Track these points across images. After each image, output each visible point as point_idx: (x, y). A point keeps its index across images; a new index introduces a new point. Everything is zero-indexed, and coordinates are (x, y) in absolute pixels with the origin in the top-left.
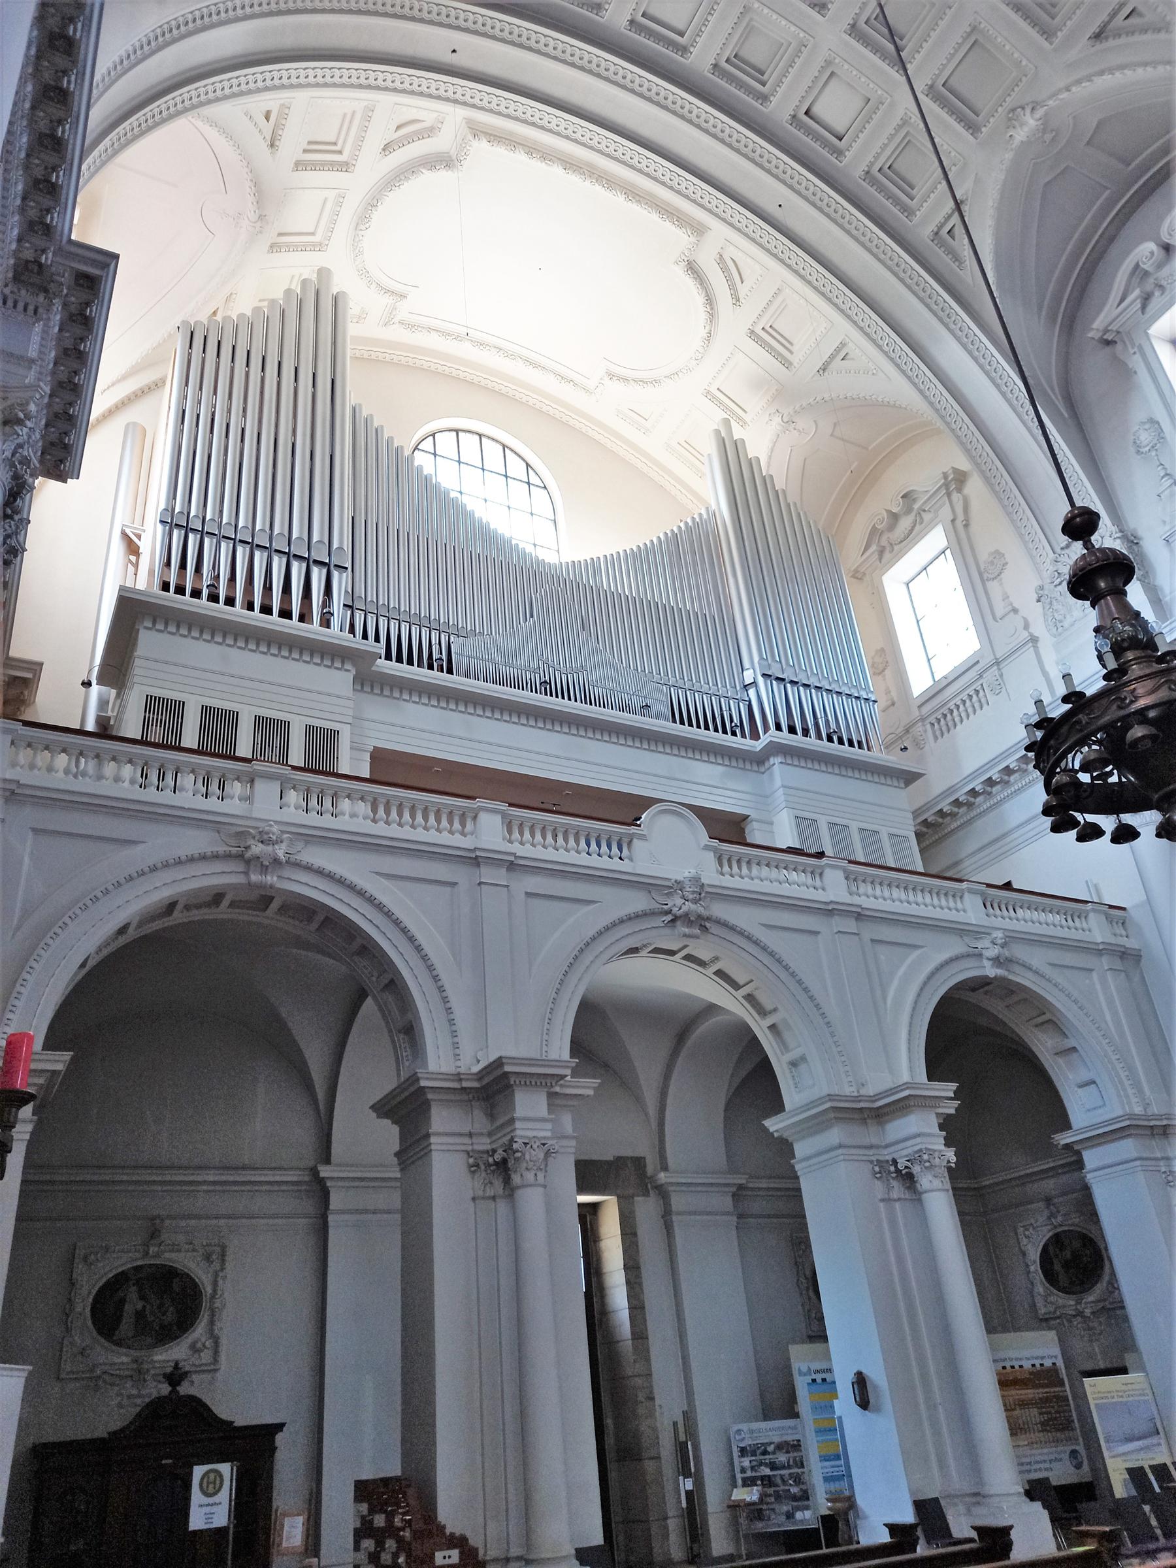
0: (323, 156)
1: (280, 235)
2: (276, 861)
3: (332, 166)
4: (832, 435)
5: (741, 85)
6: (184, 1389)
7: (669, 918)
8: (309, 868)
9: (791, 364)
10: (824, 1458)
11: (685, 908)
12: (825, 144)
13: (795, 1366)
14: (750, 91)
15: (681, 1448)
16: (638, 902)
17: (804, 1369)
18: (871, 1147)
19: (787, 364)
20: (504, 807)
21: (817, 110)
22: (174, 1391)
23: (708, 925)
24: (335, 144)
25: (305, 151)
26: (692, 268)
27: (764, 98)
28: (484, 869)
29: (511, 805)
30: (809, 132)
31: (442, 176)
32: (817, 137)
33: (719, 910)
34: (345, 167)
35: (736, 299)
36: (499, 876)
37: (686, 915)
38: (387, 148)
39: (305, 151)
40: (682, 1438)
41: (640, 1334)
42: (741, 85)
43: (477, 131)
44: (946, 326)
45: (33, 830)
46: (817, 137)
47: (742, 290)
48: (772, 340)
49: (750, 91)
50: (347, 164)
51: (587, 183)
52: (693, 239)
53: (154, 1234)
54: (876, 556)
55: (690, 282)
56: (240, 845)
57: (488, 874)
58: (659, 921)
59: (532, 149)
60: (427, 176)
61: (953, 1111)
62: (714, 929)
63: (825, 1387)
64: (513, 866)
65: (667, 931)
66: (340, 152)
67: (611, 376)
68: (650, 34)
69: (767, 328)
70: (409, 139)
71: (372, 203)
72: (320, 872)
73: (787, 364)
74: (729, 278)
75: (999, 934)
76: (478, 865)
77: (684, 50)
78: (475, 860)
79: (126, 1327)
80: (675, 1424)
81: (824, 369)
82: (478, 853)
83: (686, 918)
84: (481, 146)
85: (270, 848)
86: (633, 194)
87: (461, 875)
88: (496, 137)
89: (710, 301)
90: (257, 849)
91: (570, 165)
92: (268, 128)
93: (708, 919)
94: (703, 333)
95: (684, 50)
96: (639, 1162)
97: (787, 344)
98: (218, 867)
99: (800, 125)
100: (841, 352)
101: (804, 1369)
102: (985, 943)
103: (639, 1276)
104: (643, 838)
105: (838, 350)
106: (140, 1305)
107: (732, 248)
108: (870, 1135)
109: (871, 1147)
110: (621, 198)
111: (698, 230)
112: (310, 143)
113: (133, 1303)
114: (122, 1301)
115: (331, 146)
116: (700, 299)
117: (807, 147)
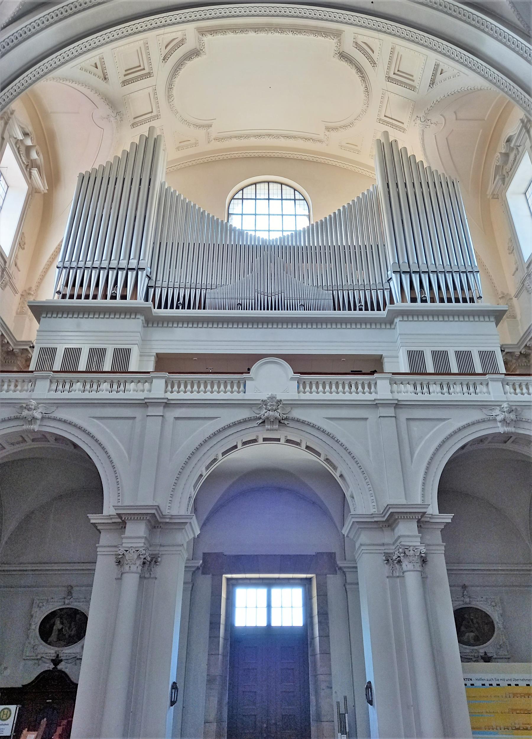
0: (135, 74)
1: (135, 118)
2: (34, 418)
3: (141, 77)
4: (456, 119)
6: (59, 667)
7: (260, 421)
8: (55, 419)
11: (266, 415)
15: (342, 717)
16: (244, 414)
18: (383, 545)
19: (412, 88)
20: (167, 375)
22: (55, 668)
23: (286, 422)
24: (140, 66)
25: (125, 75)
26: (343, 56)
28: (150, 409)
29: (169, 373)
31: (196, 60)
33: (296, 413)
34: (149, 75)
35: (373, 63)
36: (159, 411)
37: (268, 418)
39: (125, 75)
40: (342, 711)
43: (202, 32)
44: (483, 31)
47: (375, 56)
48: (399, 78)
50: (149, 73)
51: (270, 34)
52: (336, 40)
53: (70, 593)
54: (500, 182)
55: (344, 64)
56: (21, 411)
57: (151, 411)
58: (255, 424)
59: (234, 29)
60: (189, 64)
61: (450, 521)
62: (292, 424)
64: (167, 404)
65: (260, 428)
66: (144, 69)
67: (328, 129)
69: (396, 72)
70: (174, 49)
71: (170, 87)
72: (60, 420)
73: (412, 88)
74: (365, 53)
75: (505, 405)
76: (148, 406)
80: (338, 703)
81: (432, 83)
82: (146, 401)
83: (275, 418)
84: (208, 39)
85: (30, 413)
86: (296, 30)
87: (137, 413)
88: (213, 31)
89: (360, 70)
90: (25, 413)
91: (257, 29)
92: (99, 71)
93: (286, 419)
94: (362, 88)
96: (331, 556)
97: (410, 76)
100: (437, 70)
102: (497, 412)
103: (327, 619)
104: (251, 379)
105: (435, 70)
106: (60, 627)
107: (359, 36)
108: (387, 537)
109: (383, 545)
110: (290, 34)
111: (337, 34)
112: (126, 71)
114: (54, 624)
115: (139, 68)
116: (354, 71)
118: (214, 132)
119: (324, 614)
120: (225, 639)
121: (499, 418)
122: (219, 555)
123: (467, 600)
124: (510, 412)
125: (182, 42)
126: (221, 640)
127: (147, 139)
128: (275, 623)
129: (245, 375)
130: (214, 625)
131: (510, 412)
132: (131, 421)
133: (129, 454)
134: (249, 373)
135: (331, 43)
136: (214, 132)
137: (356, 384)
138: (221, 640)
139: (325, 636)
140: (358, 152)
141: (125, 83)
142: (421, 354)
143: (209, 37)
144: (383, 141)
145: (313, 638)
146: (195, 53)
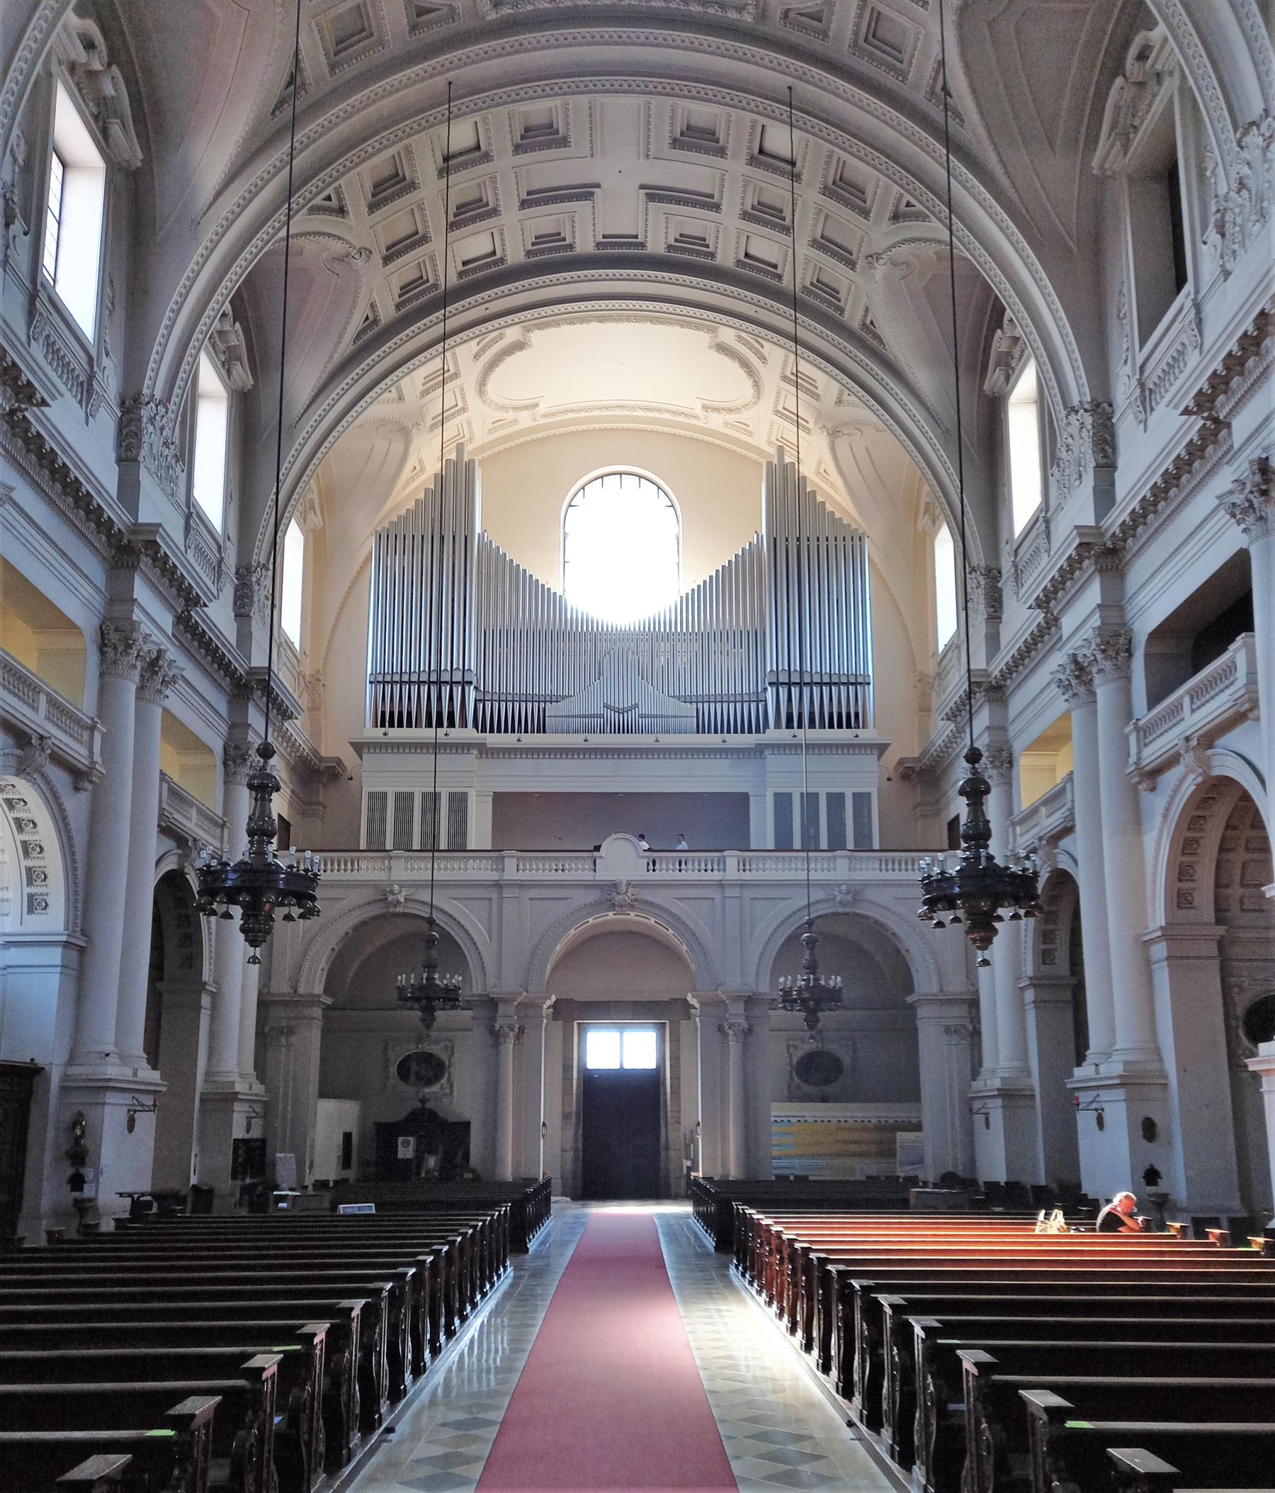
2: (399, 903)
5: (691, 252)
8: (417, 901)
9: (819, 396)
12: (767, 273)
14: (698, 253)
21: (751, 252)
26: (722, 348)
27: (712, 255)
30: (752, 268)
31: (518, 355)
32: (760, 270)
41: (676, 1091)
42: (691, 252)
46: (760, 270)
49: (698, 253)
60: (509, 362)
67: (705, 408)
68: (613, 245)
74: (751, 348)
77: (642, 245)
79: (412, 1078)
95: (642, 245)
98: (370, 908)
99: (744, 265)
113: (414, 1067)
116: (736, 365)
117: (755, 278)
118: (542, 409)
119: (675, 1059)
120: (578, 1080)
121: (838, 899)
122: (571, 1001)
124: (848, 893)
125: (501, 337)
126: (575, 1082)
127: (456, 464)
128: (626, 1067)
129: (596, 854)
130: (567, 1068)
131: (848, 893)
135: (704, 338)
136: (542, 409)
137: (706, 860)
138: (575, 1082)
139: (676, 1077)
140: (751, 434)
143: (537, 332)
144: (775, 461)
145: (665, 1079)
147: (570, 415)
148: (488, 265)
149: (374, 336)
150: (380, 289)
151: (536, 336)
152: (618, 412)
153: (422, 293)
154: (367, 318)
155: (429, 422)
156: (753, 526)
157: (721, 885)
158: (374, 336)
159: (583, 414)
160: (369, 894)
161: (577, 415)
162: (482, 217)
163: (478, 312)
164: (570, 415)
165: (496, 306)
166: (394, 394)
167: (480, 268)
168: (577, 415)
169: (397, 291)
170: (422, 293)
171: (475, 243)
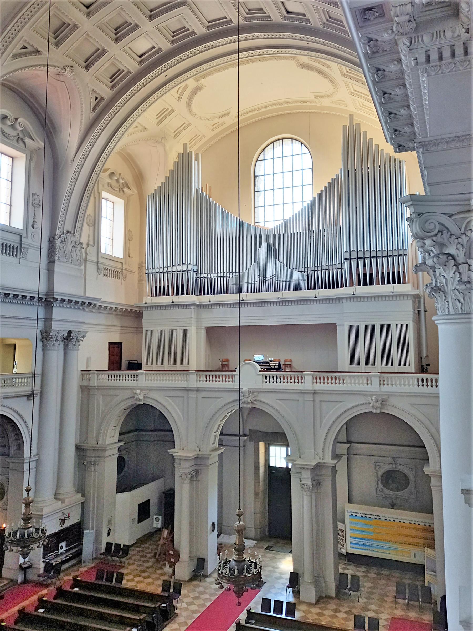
8: (149, 398)
10: (351, 537)
13: (346, 510)
17: (349, 511)
25: (157, 118)
31: (199, 93)
34: (173, 110)
38: (179, 98)
39: (157, 118)
45: (103, 395)
63: (356, 517)
64: (198, 390)
71: (190, 111)
78: (187, 390)
101: (349, 511)
112: (157, 115)
123: (394, 466)
125: (186, 86)
132: (182, 398)
133: (183, 417)
134: (235, 371)
141: (159, 123)
142: (357, 327)
146: (198, 89)
147: (250, 114)
148: (154, 54)
149: (102, 108)
150: (96, 82)
151: (203, 81)
152: (274, 107)
153: (123, 78)
154: (97, 98)
155: (173, 135)
156: (336, 168)
157: (302, 392)
158: (102, 108)
159: (256, 112)
160: (128, 394)
161: (254, 113)
162: (131, 31)
163: (161, 79)
164: (250, 114)
165: (171, 73)
166: (140, 128)
167: (150, 56)
168: (254, 113)
169: (108, 81)
170: (123, 78)
171: (142, 45)
